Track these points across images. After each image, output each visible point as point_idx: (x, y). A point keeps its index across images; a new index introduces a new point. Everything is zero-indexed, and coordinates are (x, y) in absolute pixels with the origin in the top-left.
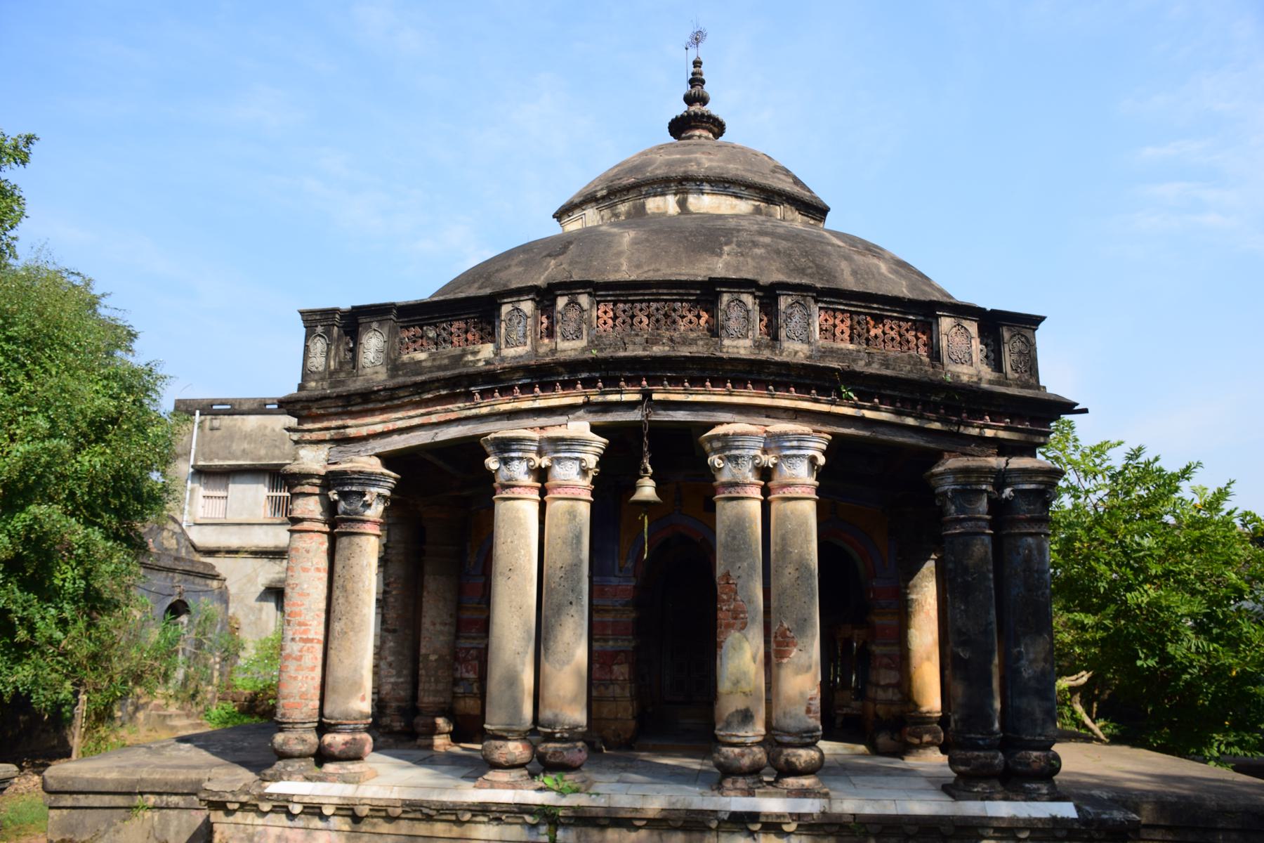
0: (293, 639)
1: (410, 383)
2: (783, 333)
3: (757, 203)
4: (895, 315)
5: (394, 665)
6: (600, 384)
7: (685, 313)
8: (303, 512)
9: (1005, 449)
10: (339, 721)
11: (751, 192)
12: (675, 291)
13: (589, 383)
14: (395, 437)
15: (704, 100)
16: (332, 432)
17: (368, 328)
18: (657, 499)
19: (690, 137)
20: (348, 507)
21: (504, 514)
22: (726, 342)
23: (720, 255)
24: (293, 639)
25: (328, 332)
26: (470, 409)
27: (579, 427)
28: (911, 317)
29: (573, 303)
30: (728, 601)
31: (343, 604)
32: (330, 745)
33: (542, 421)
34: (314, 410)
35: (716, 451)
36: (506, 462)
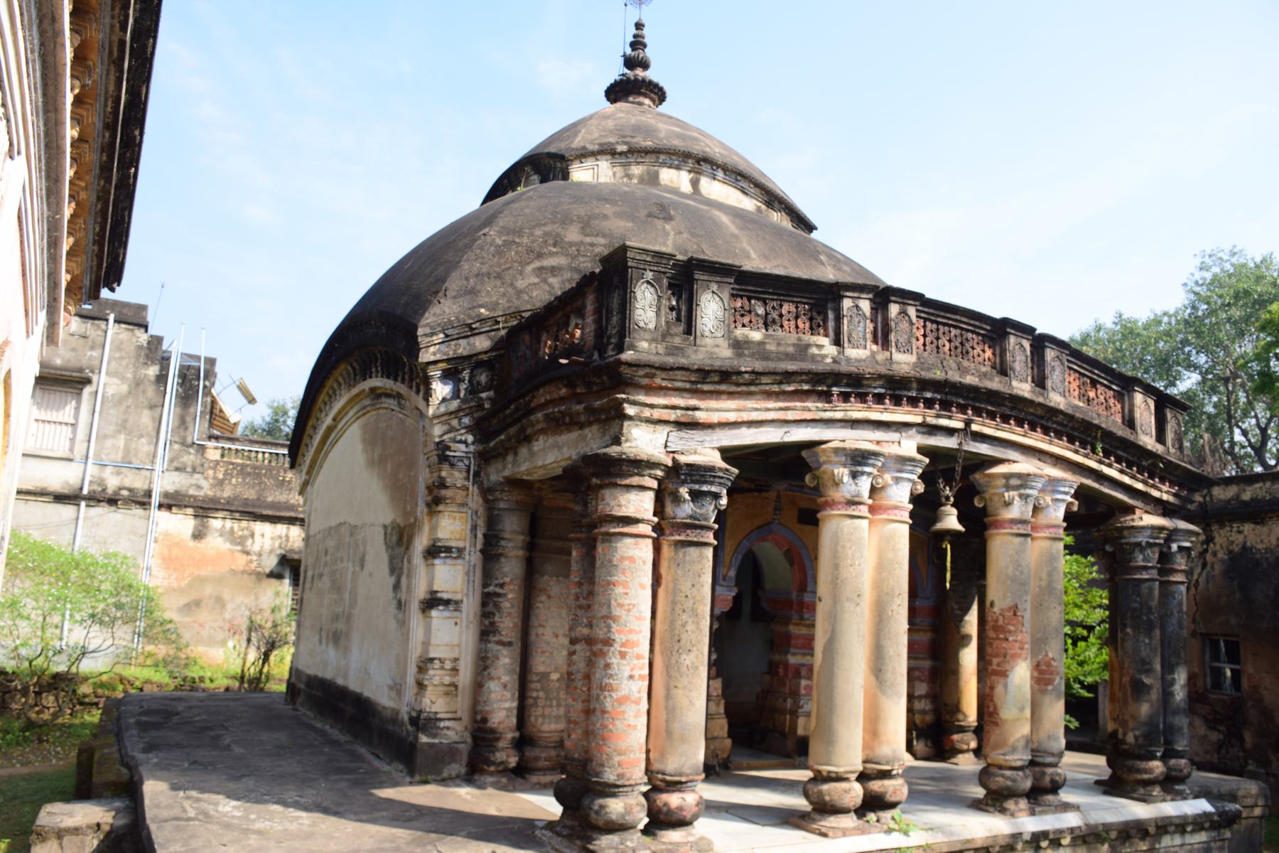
0: (631, 677)
1: (780, 371)
3: (759, 204)
4: (1105, 382)
5: (509, 686)
6: (937, 406)
7: (975, 346)
8: (638, 511)
10: (691, 777)
11: (758, 190)
12: (972, 322)
13: (929, 404)
14: (744, 430)
15: (645, 65)
16: (679, 412)
18: (960, 527)
19: (640, 104)
20: (698, 511)
21: (852, 534)
24: (631, 677)
26: (825, 411)
28: (1114, 387)
30: (1015, 632)
31: (693, 632)
32: (680, 808)
34: (658, 381)
36: (854, 475)
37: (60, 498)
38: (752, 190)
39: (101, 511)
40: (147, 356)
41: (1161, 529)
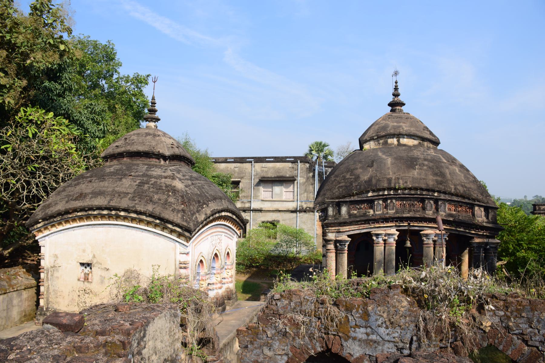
2: (439, 210)
9: (487, 237)
13: (396, 221)
17: (343, 205)
22: (427, 212)
23: (415, 169)
25: (333, 206)
27: (393, 231)
29: (391, 202)
33: (385, 229)
35: (424, 237)
36: (377, 238)
37: (292, 212)
38: (416, 138)
39: (302, 214)
40: (309, 171)
41: (482, 243)
